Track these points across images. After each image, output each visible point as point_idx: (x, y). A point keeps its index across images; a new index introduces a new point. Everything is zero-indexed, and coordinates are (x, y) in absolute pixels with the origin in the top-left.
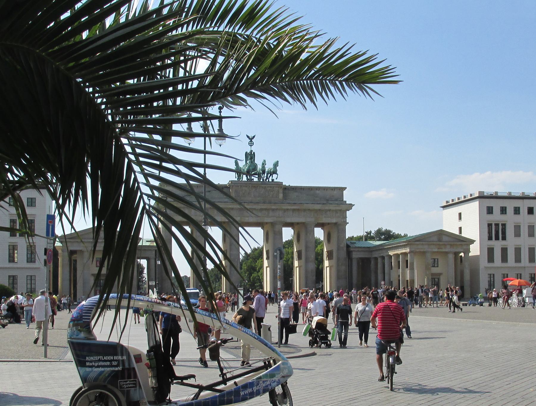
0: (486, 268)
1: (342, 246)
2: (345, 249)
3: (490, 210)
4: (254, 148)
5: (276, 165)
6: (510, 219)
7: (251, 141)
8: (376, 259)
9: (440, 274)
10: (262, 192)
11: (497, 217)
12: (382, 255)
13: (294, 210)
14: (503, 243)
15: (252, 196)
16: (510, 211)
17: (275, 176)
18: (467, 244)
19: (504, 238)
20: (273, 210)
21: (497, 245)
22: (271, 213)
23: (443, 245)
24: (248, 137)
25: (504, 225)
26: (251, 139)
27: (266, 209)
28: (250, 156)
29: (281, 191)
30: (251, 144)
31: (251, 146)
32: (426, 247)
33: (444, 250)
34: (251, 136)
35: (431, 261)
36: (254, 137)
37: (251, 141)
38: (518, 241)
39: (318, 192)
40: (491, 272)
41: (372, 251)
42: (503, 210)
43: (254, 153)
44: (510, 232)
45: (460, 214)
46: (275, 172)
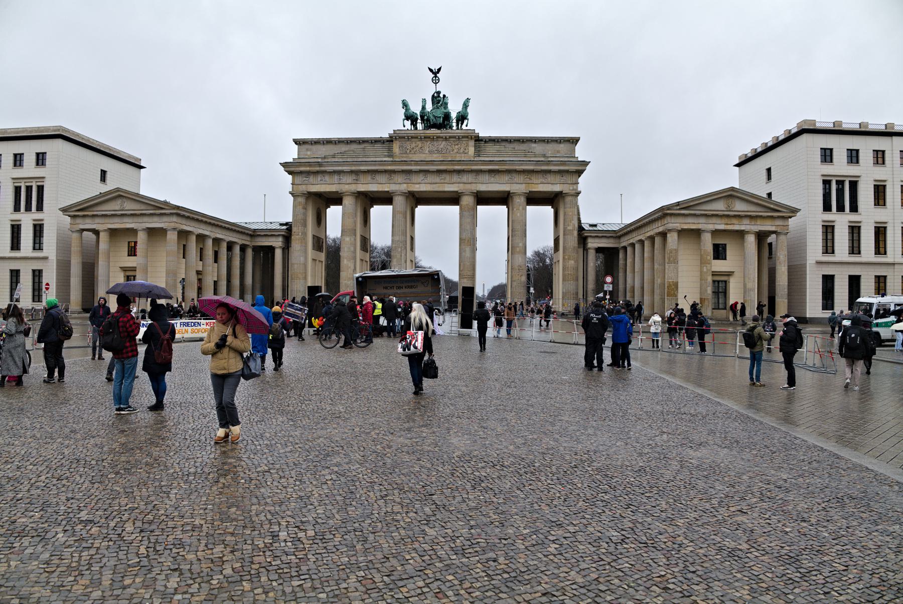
0: (819, 263)
1: (569, 228)
2: (576, 233)
3: (827, 155)
4: (443, 88)
5: (466, 105)
6: (867, 174)
7: (436, 77)
8: (625, 248)
9: (730, 274)
10: (442, 146)
11: (840, 167)
12: (631, 241)
13: (491, 172)
14: (854, 217)
16: (867, 157)
18: (783, 217)
19: (854, 208)
20: (459, 172)
21: (842, 222)
22: (455, 178)
23: (735, 216)
24: (431, 70)
25: (854, 185)
26: (435, 73)
27: (445, 171)
28: (438, 99)
29: (472, 143)
31: (436, 83)
32: (702, 220)
33: (737, 227)
34: (435, 67)
35: (709, 248)
36: (439, 70)
37: (436, 77)
38: (881, 215)
39: (534, 145)
40: (828, 271)
41: (619, 237)
42: (853, 156)
43: (444, 96)
44: (866, 195)
45: (769, 170)
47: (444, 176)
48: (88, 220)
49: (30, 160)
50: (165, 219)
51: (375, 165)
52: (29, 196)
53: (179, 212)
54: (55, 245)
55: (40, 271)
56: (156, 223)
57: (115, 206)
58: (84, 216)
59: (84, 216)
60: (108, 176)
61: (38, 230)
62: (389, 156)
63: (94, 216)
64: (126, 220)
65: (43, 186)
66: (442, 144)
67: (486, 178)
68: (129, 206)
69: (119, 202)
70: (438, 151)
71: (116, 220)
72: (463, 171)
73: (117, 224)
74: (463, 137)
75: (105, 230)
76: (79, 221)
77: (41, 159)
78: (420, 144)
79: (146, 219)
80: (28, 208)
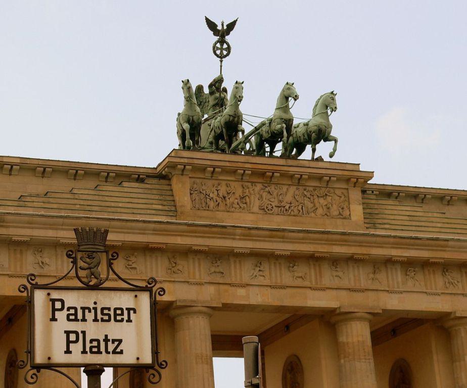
5: (328, 104)
7: (222, 41)
10: (289, 198)
13: (409, 265)
15: (256, 209)
17: (323, 149)
20: (335, 261)
22: (328, 277)
24: (211, 25)
26: (222, 33)
30: (222, 50)
31: (221, 57)
34: (221, 21)
36: (231, 26)
37: (222, 41)
46: (321, 134)
47: (302, 269)
51: (143, 232)
62: (167, 213)
66: (290, 193)
67: (397, 277)
70: (283, 210)
72: (352, 260)
74: (339, 179)
78: (237, 188)
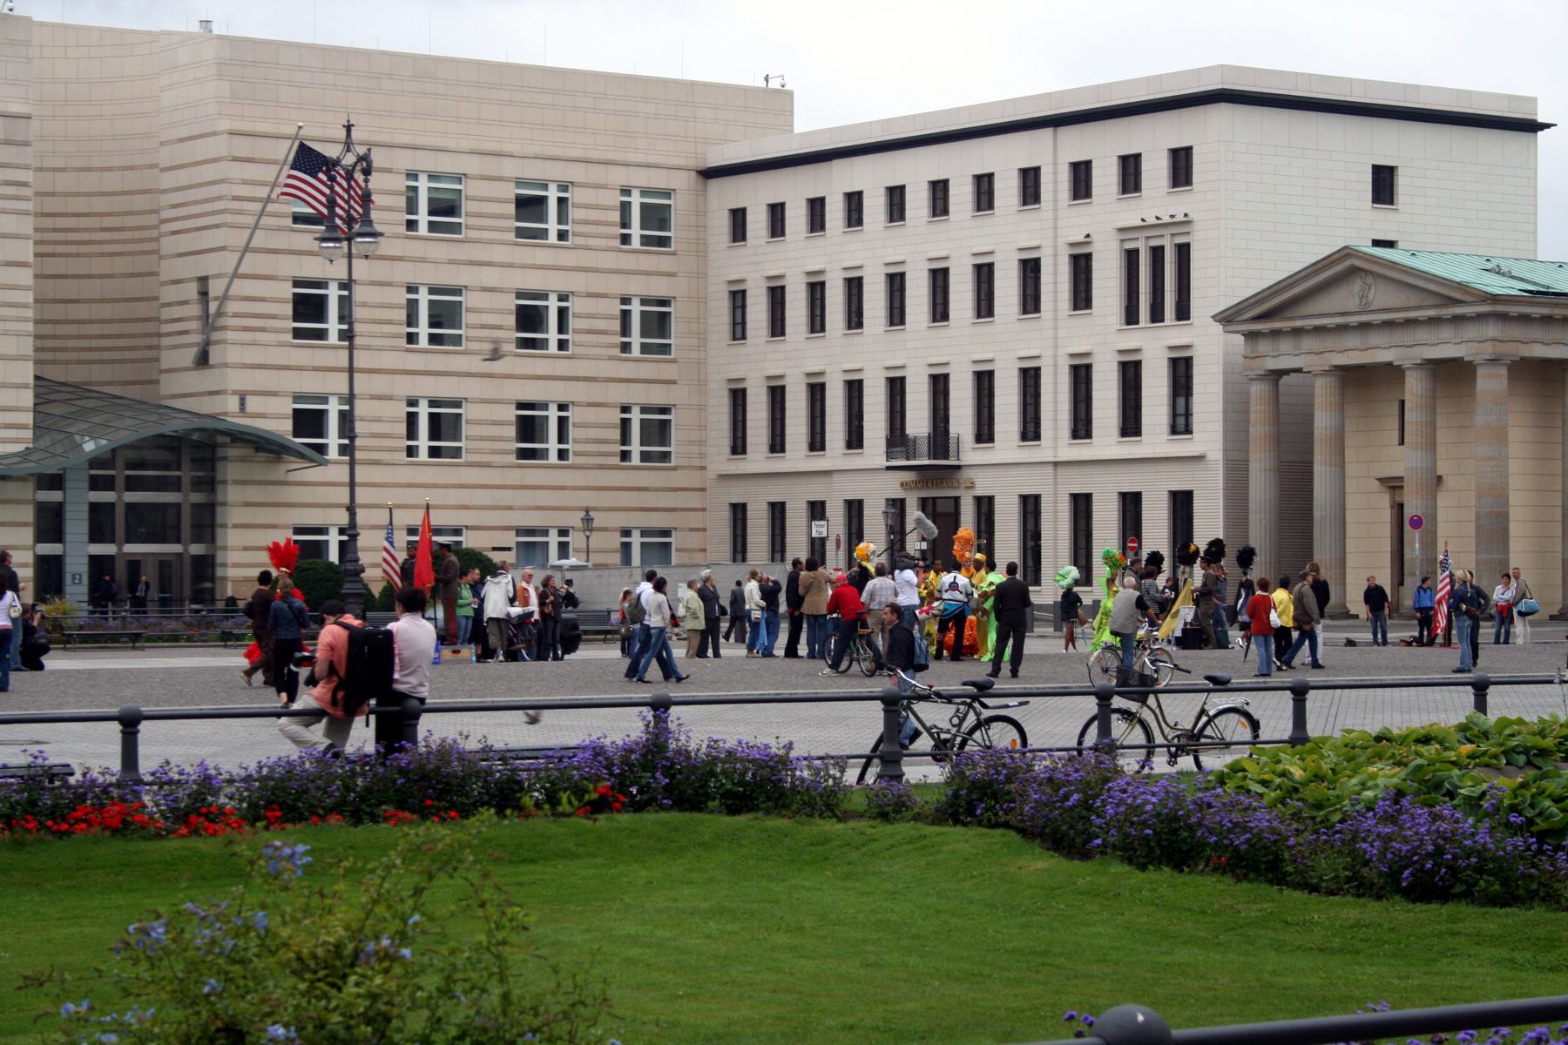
48: (1285, 345)
49: (1156, 170)
50: (1471, 331)
52: (1159, 277)
53: (1500, 308)
54: (1220, 417)
55: (1188, 495)
56: (1447, 345)
57: (1344, 300)
58: (1275, 334)
59: (1275, 334)
60: (1402, 183)
61: (1181, 372)
63: (1297, 332)
64: (1376, 338)
65: (1188, 245)
68: (1383, 298)
69: (1356, 285)
71: (1352, 340)
73: (1353, 352)
75: (1325, 373)
76: (1264, 346)
77: (1181, 166)
79: (1422, 334)
80: (1157, 315)
